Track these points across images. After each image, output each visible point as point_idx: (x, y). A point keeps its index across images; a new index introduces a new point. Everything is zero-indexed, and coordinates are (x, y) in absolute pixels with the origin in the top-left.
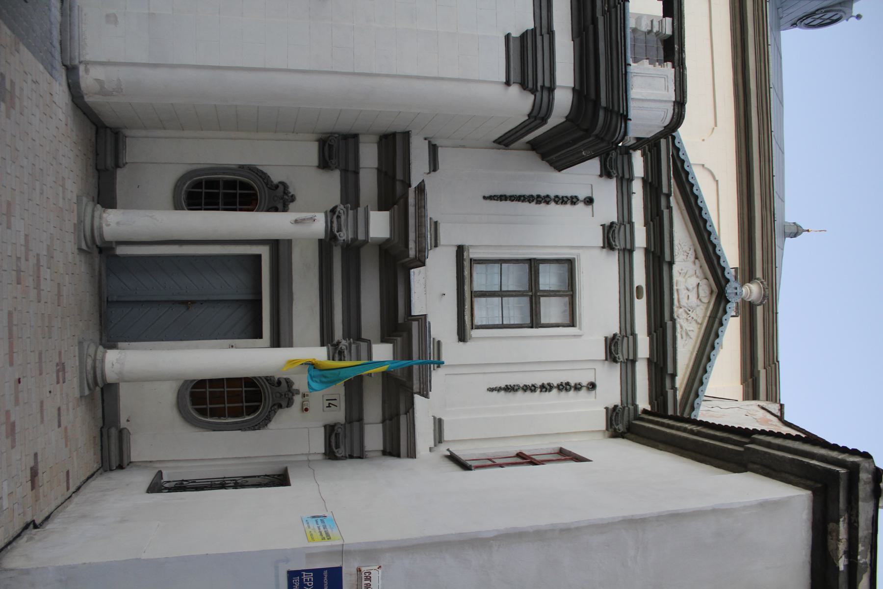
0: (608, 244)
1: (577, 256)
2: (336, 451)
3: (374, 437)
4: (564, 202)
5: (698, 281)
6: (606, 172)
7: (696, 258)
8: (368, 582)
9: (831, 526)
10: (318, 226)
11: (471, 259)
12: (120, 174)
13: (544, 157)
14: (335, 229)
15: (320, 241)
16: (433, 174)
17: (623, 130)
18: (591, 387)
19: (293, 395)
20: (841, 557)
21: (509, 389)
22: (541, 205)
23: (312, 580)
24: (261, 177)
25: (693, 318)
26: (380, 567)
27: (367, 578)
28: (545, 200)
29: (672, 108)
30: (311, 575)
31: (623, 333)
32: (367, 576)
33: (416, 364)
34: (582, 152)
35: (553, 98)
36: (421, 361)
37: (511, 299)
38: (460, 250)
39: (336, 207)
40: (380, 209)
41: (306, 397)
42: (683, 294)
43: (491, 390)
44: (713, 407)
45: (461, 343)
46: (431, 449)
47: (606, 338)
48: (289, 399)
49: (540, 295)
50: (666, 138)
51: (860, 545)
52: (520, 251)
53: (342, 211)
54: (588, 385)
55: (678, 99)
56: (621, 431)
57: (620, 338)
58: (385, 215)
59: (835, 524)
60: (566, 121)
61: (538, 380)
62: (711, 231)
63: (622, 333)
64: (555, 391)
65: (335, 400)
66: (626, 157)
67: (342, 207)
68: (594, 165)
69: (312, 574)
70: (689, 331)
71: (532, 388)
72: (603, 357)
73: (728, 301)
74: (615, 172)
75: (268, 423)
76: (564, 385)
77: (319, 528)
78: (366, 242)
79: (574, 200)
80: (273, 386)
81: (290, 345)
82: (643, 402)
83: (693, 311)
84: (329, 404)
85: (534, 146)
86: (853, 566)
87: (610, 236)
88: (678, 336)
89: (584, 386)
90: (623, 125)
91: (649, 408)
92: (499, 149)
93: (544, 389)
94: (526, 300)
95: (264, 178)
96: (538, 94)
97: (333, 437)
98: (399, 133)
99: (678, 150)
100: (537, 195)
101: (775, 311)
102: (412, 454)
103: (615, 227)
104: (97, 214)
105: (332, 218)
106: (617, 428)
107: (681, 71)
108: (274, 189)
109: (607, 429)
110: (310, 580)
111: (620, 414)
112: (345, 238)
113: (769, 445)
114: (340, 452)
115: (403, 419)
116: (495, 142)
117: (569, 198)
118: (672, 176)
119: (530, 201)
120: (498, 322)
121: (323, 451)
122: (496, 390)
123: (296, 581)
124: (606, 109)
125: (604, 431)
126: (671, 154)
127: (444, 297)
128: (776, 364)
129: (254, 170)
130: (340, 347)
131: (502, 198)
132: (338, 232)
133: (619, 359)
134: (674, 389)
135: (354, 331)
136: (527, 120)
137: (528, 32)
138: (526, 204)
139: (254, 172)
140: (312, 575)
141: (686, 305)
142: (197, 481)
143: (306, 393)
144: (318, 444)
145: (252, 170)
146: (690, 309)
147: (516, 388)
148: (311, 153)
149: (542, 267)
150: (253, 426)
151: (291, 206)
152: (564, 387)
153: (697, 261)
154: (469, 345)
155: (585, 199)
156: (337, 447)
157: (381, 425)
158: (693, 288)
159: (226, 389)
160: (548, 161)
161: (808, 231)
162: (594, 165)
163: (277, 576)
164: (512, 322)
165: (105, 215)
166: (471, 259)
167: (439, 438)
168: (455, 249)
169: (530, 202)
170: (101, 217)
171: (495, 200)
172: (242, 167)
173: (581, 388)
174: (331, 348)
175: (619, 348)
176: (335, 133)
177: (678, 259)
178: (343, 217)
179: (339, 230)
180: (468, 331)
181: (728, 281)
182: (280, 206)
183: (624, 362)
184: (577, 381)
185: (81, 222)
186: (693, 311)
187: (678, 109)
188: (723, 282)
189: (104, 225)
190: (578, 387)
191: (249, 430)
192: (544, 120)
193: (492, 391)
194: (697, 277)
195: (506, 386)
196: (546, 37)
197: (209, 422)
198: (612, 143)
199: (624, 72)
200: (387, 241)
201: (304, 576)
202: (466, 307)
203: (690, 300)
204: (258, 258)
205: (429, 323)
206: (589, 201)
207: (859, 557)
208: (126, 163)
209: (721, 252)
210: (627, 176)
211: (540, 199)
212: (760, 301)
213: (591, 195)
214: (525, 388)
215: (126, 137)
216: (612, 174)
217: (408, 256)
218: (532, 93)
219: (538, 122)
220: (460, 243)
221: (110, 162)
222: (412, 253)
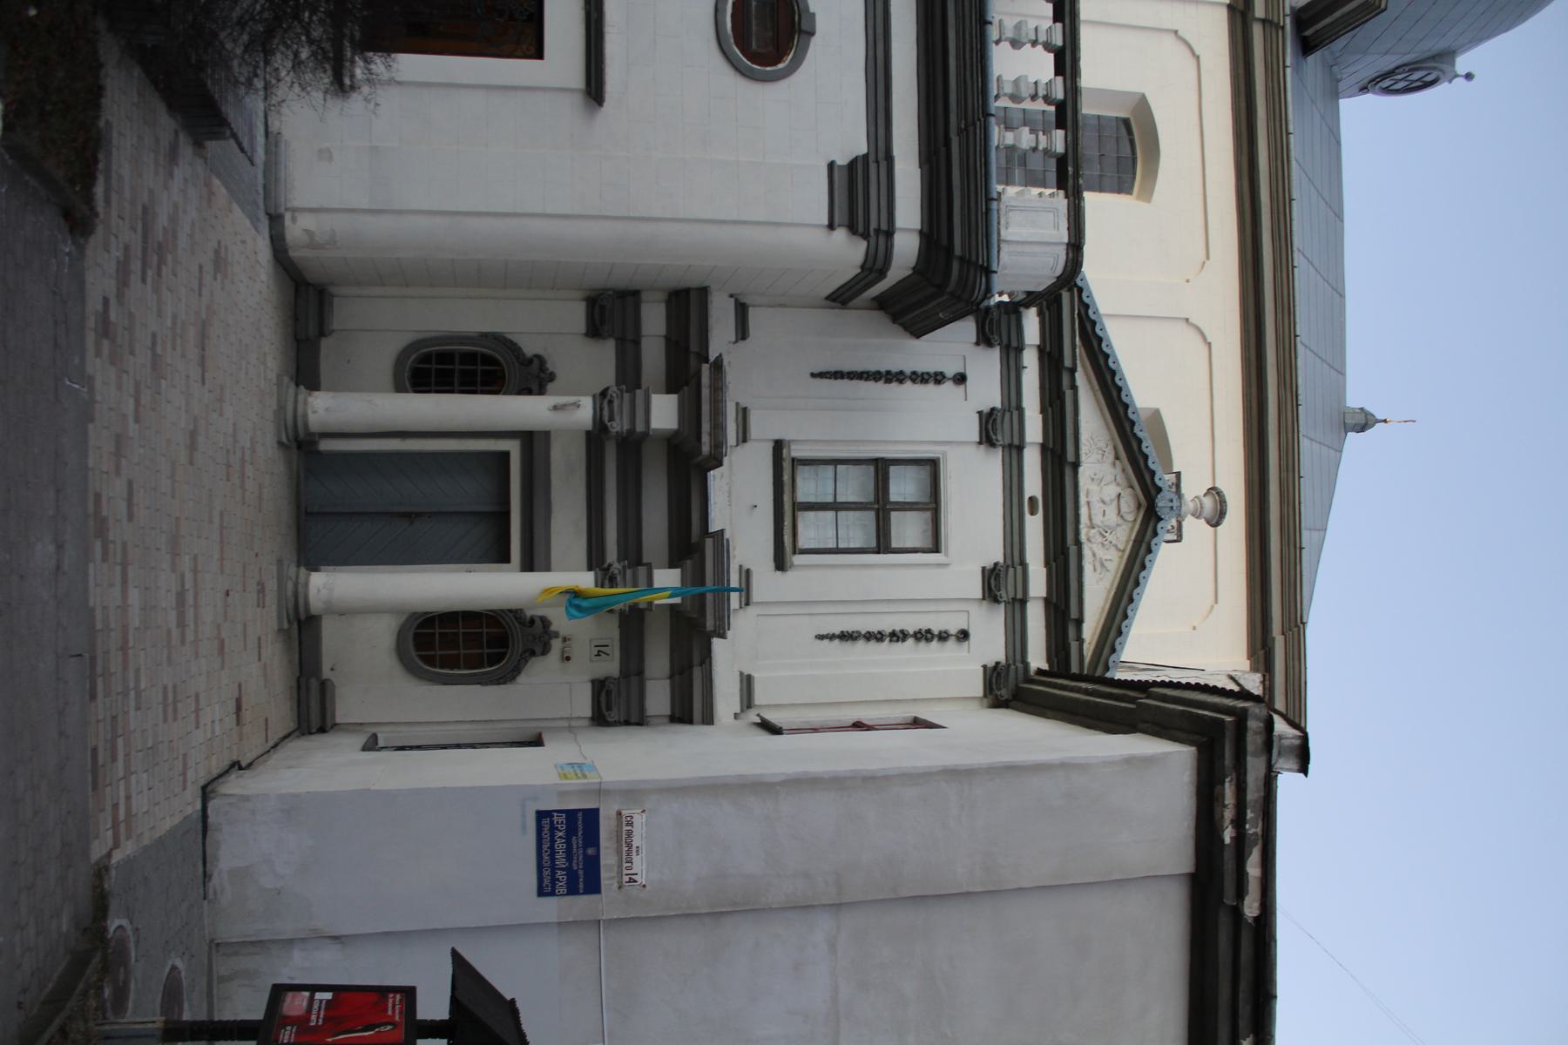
0: (987, 438)
2: (607, 714)
3: (658, 697)
5: (1118, 490)
6: (984, 339)
7: (1117, 458)
8: (630, 828)
10: (585, 413)
12: (325, 344)
13: (896, 318)
14: (606, 418)
15: (588, 433)
16: (741, 343)
17: (983, 287)
18: (962, 636)
19: (550, 639)
20: (1227, 827)
21: (845, 636)
22: (892, 385)
24: (509, 348)
25: (1111, 542)
26: (644, 811)
28: (897, 377)
29: (1065, 252)
31: (1009, 562)
33: (710, 591)
34: (938, 313)
35: (892, 246)
36: (716, 587)
37: (851, 514)
38: (778, 446)
39: (607, 389)
40: (669, 391)
41: (567, 642)
42: (1097, 508)
43: (821, 637)
45: (779, 573)
46: (736, 716)
47: (984, 569)
50: (1070, 290)
51: (1249, 811)
52: (862, 448)
53: (614, 395)
54: (958, 632)
55: (1073, 241)
56: (1003, 699)
58: (673, 398)
61: (887, 624)
62: (1135, 420)
64: (910, 641)
65: (607, 646)
66: (1013, 317)
67: (615, 389)
68: (966, 329)
70: (1106, 560)
71: (878, 637)
72: (980, 596)
73: (1159, 519)
74: (996, 338)
75: (516, 676)
76: (923, 632)
77: (575, 771)
78: (646, 434)
79: (939, 378)
81: (548, 569)
82: (1037, 658)
83: (1111, 533)
84: (599, 651)
85: (882, 304)
86: (1240, 838)
87: (990, 427)
89: (952, 635)
90: (984, 280)
92: (833, 308)
93: (895, 638)
94: (871, 515)
96: (873, 240)
97: (603, 694)
98: (693, 289)
99: (1087, 307)
101: (1298, 546)
102: (708, 719)
104: (301, 398)
105: (602, 404)
106: (999, 693)
107: (1077, 202)
109: (985, 696)
111: (1003, 675)
112: (618, 429)
113: (1165, 698)
115: (697, 673)
116: (827, 298)
120: (832, 545)
121: (589, 714)
124: (961, 259)
126: (1076, 312)
127: (756, 509)
128: (1299, 627)
130: (611, 570)
131: (838, 375)
132: (609, 421)
133: (1001, 597)
134: (1080, 640)
135: (633, 554)
137: (859, 159)
138: (871, 384)
141: (1100, 524)
146: (1107, 530)
147: (855, 635)
148: (575, 315)
149: (894, 471)
151: (550, 386)
152: (924, 636)
154: (790, 575)
155: (955, 376)
156: (609, 708)
157: (668, 681)
158: (1112, 501)
160: (901, 324)
161: (1385, 421)
162: (966, 329)
163: (524, 816)
164: (852, 546)
165: (310, 399)
166: (793, 460)
167: (747, 700)
168: (770, 446)
169: (876, 380)
170: (306, 403)
171: (826, 378)
172: (484, 335)
174: (599, 573)
176: (608, 290)
177: (1083, 458)
178: (616, 403)
179: (611, 419)
182: (535, 387)
184: (943, 628)
185: (281, 408)
187: (1073, 253)
188: (1153, 492)
189: (309, 412)
190: (943, 637)
192: (882, 273)
193: (822, 639)
194: (1118, 485)
195: (842, 632)
196: (883, 165)
197: (438, 673)
198: (972, 303)
199: (984, 210)
200: (676, 433)
202: (786, 524)
203: (1106, 518)
204: (505, 456)
205: (728, 540)
206: (961, 379)
207: (1247, 826)
208: (333, 331)
210: (1014, 344)
211: (889, 377)
212: (1215, 520)
213: (962, 371)
214: (868, 635)
215: (333, 296)
216: (993, 341)
217: (700, 452)
219: (873, 275)
220: (777, 437)
222: (706, 449)
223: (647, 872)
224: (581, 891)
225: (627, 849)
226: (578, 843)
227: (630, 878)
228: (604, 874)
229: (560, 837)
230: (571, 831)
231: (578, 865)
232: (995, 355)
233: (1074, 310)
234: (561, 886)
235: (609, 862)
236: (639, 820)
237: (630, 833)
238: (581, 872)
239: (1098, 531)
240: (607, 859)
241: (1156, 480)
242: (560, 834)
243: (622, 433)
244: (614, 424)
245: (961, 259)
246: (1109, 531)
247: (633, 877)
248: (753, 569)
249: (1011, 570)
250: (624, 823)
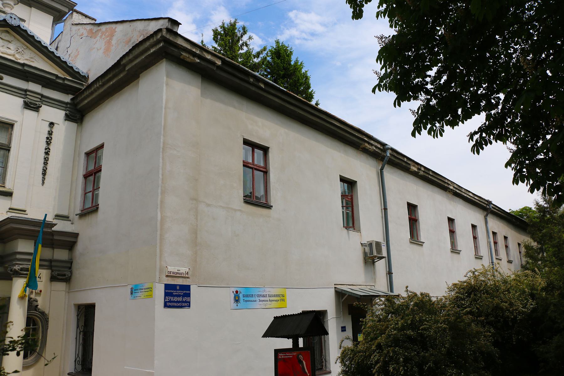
2: (67, 276)
9: (182, 57)
25: (22, 50)
31: (23, 96)
33: (43, 229)
44: (67, 52)
59: (182, 56)
82: (67, 98)
83: (18, 48)
84: (38, 277)
91: (71, 97)
102: (76, 235)
106: (78, 118)
110: (168, 298)
113: (131, 61)
114: (68, 274)
121: (65, 283)
123: (168, 304)
125: (78, 125)
134: (64, 79)
142: (77, 353)
144: (61, 286)
146: (16, 50)
156: (64, 275)
157: (55, 250)
167: (65, 218)
173: (52, 131)
180: (5, 190)
183: (43, 102)
184: (47, 132)
186: (18, 48)
190: (50, 133)
191: (48, 324)
195: (43, 174)
203: (11, 48)
228: (185, 284)
235: (181, 281)
236: (171, 269)
237: (174, 273)
238: (184, 292)
240: (180, 282)
242: (172, 299)
246: (18, 49)
248: (9, 207)
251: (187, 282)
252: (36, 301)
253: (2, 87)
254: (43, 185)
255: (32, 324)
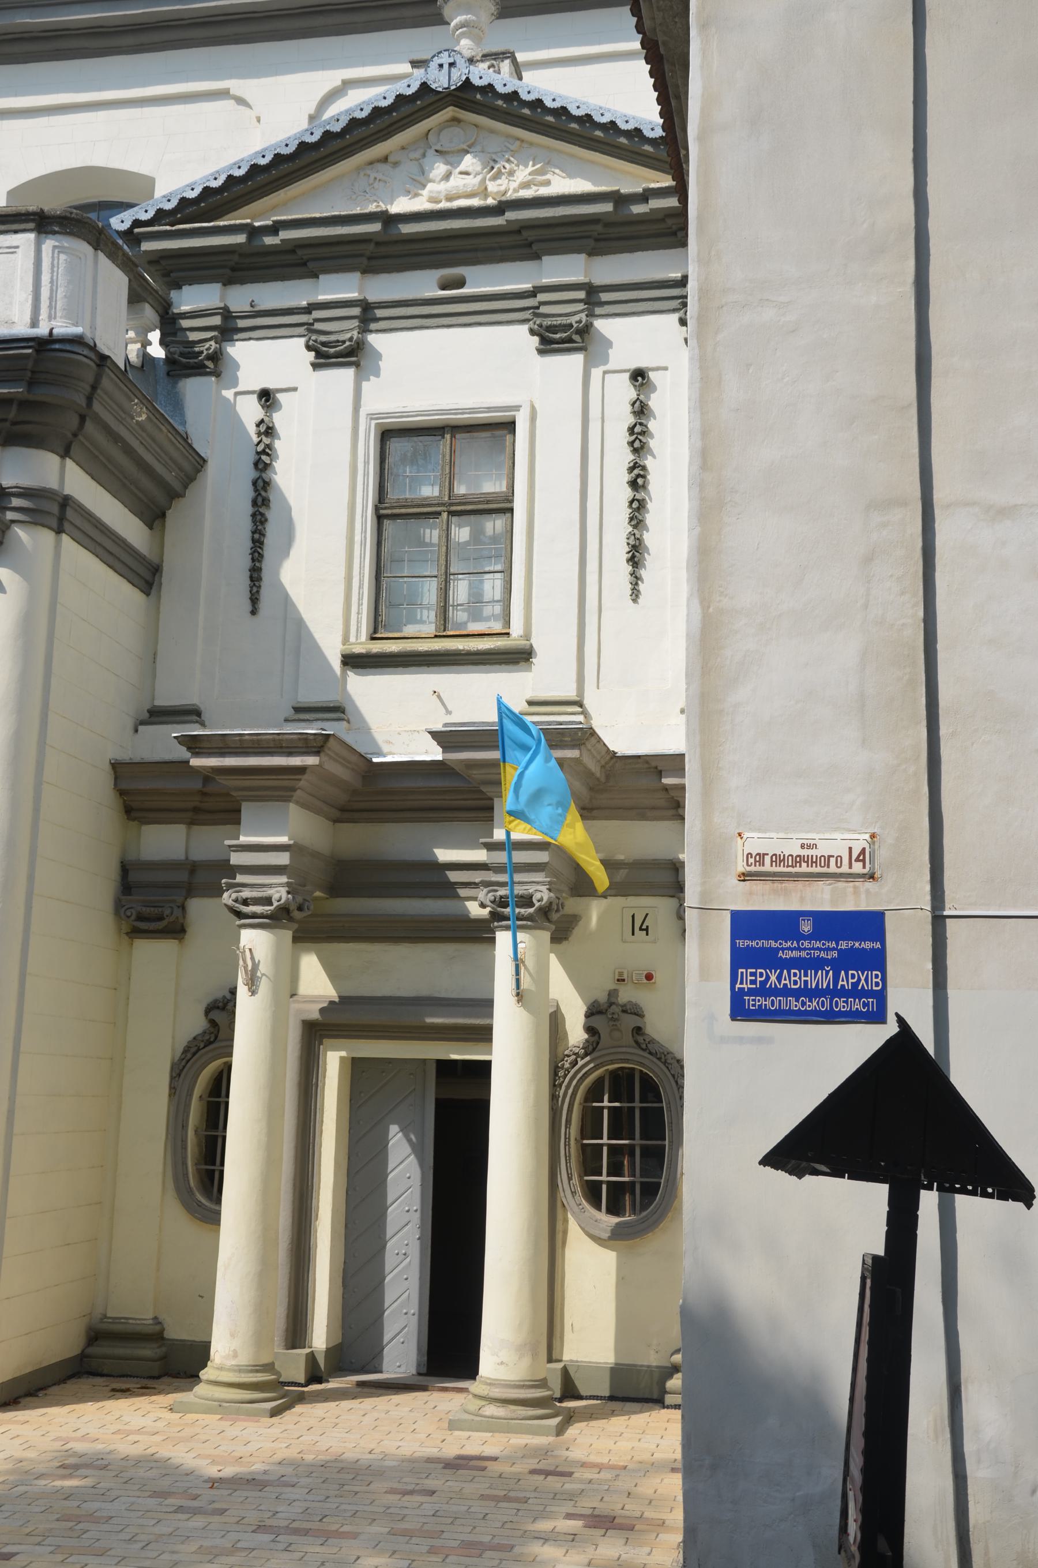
1: (372, 419)
4: (267, 450)
5: (431, 153)
7: (385, 159)
8: (767, 859)
11: (373, 639)
13: (174, 495)
15: (296, 939)
16: (205, 716)
17: (68, 347)
18: (640, 379)
21: (633, 557)
22: (271, 498)
23: (754, 970)
24: (194, 1054)
26: (740, 835)
27: (759, 861)
30: (742, 973)
31: (527, 315)
32: (756, 861)
34: (137, 421)
41: (625, 977)
42: (457, 182)
43: (635, 594)
48: (624, 1011)
49: (450, 496)
53: (234, 896)
54: (635, 386)
55: (32, 225)
57: (538, 322)
60: (70, 458)
63: (530, 317)
65: (633, 916)
67: (226, 895)
69: (740, 970)
71: (638, 509)
74: (207, 345)
80: (598, 1043)
84: (641, 929)
87: (332, 350)
88: (544, 191)
90: (57, 346)
92: (161, 584)
93: (640, 481)
95: (196, 1048)
100: (253, 506)
103: (315, 341)
108: (217, 1027)
110: (752, 974)
116: (148, 594)
117: (260, 438)
118: (211, 224)
119: (263, 519)
122: (637, 584)
123: (752, 1002)
126: (168, 228)
129: (181, 1068)
132: (271, 904)
133: (580, 322)
134: (645, 196)
136: (66, 534)
139: (184, 1067)
140: (744, 970)
141: (479, 178)
143: (617, 977)
145: (182, 1070)
147: (632, 541)
150: (679, 1089)
153: (390, 159)
154: (536, 642)
155: (263, 407)
159: (605, 1140)
160: (186, 487)
171: (258, 592)
172: (173, 1090)
175: (559, 322)
178: (246, 893)
179: (268, 901)
180: (509, 642)
181: (424, 87)
185: (220, 1407)
190: (641, 410)
193: (638, 591)
194: (424, 155)
195: (628, 561)
201: (744, 986)
202: (461, 647)
203: (470, 169)
208: (155, 1318)
209: (365, 107)
211: (260, 500)
213: (255, 396)
214: (633, 523)
217: (320, 766)
218: (8, 527)
221: (148, 1351)
223: (849, 831)
224: (878, 945)
225: (804, 865)
226: (789, 949)
227: (857, 860)
228: (849, 905)
229: (779, 978)
230: (769, 960)
231: (829, 949)
232: (239, 351)
233: (166, 231)
234: (868, 979)
235: (827, 896)
236: (756, 842)
237: (778, 860)
238: (843, 945)
239: (490, 180)
241: (409, 92)
242: (773, 978)
243: (288, 884)
244: (276, 896)
245: (31, 384)
246: (492, 163)
247: (854, 857)
249: (543, 310)
250: (758, 869)
251: (863, 896)
252: (635, 1014)
253: (482, 309)
254: (635, 601)
255: (606, 1097)
